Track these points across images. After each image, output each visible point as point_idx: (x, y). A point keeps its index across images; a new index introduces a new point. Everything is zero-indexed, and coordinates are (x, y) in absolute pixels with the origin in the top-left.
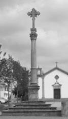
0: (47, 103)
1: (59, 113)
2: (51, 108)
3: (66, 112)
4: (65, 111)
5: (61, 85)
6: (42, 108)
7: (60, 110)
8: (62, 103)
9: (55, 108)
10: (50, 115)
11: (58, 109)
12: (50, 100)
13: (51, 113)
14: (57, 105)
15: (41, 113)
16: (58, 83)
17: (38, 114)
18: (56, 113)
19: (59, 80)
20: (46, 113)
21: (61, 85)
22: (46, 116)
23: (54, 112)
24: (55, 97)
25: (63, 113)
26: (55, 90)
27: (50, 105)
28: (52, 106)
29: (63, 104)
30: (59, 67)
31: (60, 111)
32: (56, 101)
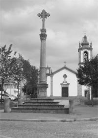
0: (55, 101)
1: (67, 111)
2: (59, 106)
3: (74, 110)
4: (72, 109)
5: (68, 84)
6: (51, 106)
7: (68, 107)
8: (70, 101)
9: (63, 106)
10: (58, 113)
11: (65, 107)
12: (58, 98)
13: (59, 111)
14: (65, 103)
15: (49, 110)
16: (66, 82)
17: (46, 111)
18: (63, 111)
19: (67, 79)
20: (55, 110)
21: (68, 84)
22: (53, 113)
23: (62, 109)
24: (63, 95)
25: (70, 110)
26: (63, 88)
27: (58, 103)
28: (60, 104)
29: (71, 102)
30: (67, 66)
31: (68, 109)
32: (63, 99)
